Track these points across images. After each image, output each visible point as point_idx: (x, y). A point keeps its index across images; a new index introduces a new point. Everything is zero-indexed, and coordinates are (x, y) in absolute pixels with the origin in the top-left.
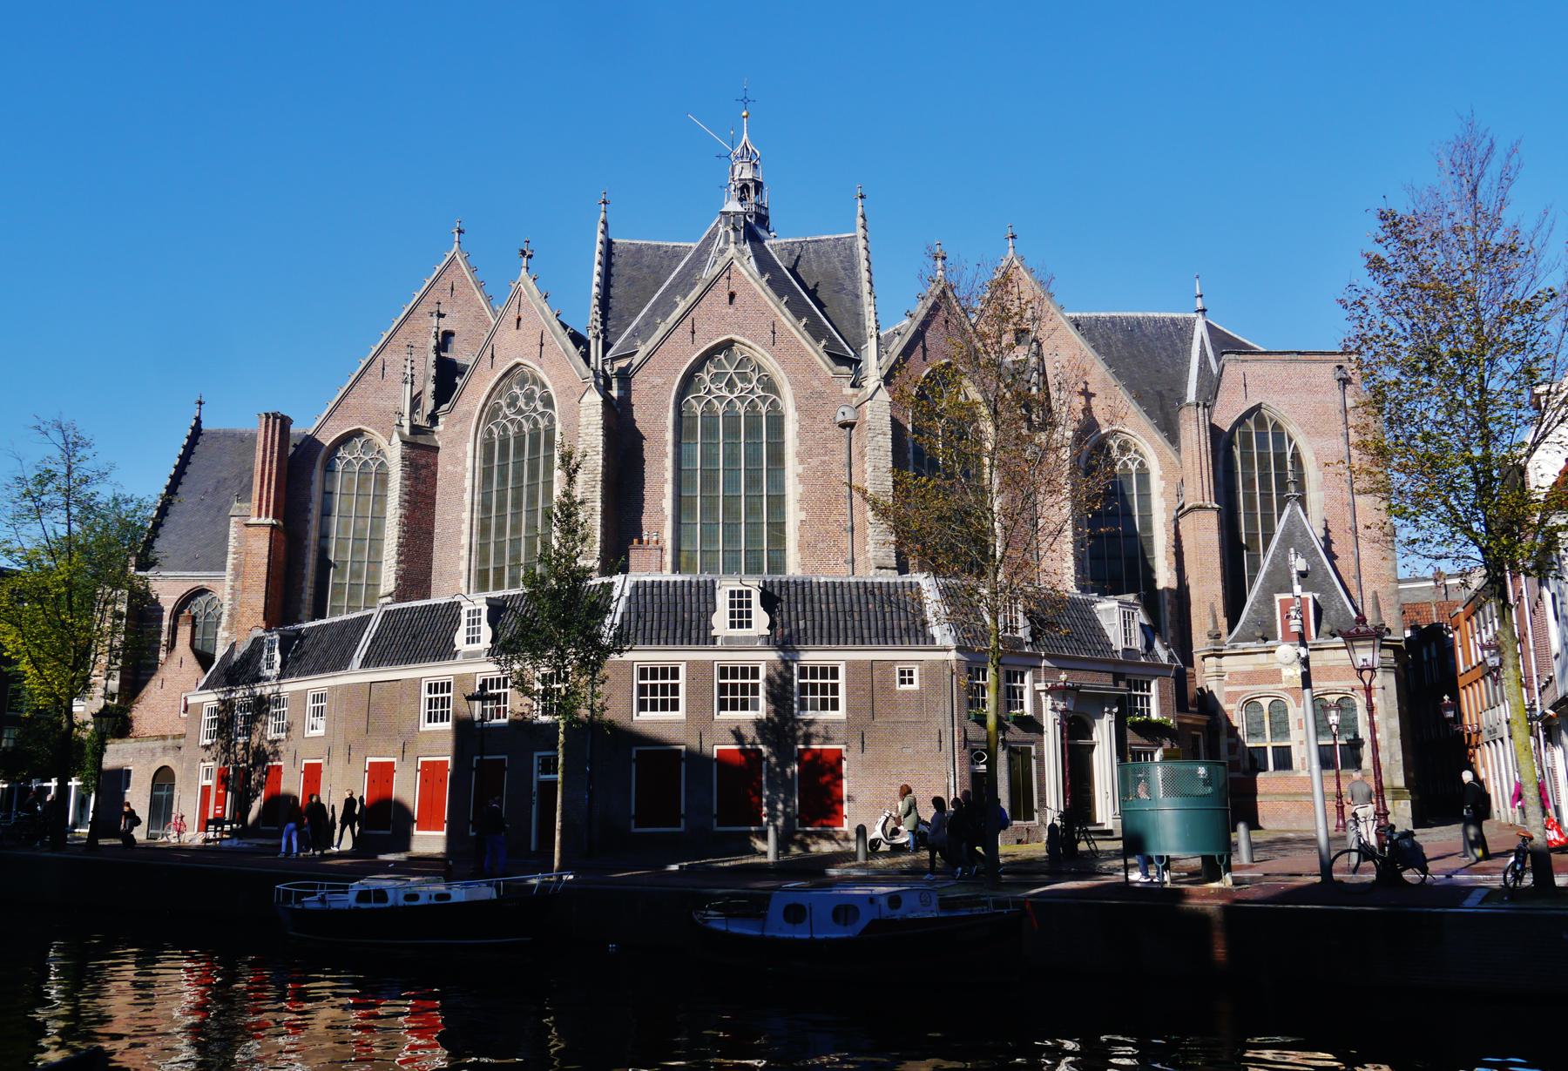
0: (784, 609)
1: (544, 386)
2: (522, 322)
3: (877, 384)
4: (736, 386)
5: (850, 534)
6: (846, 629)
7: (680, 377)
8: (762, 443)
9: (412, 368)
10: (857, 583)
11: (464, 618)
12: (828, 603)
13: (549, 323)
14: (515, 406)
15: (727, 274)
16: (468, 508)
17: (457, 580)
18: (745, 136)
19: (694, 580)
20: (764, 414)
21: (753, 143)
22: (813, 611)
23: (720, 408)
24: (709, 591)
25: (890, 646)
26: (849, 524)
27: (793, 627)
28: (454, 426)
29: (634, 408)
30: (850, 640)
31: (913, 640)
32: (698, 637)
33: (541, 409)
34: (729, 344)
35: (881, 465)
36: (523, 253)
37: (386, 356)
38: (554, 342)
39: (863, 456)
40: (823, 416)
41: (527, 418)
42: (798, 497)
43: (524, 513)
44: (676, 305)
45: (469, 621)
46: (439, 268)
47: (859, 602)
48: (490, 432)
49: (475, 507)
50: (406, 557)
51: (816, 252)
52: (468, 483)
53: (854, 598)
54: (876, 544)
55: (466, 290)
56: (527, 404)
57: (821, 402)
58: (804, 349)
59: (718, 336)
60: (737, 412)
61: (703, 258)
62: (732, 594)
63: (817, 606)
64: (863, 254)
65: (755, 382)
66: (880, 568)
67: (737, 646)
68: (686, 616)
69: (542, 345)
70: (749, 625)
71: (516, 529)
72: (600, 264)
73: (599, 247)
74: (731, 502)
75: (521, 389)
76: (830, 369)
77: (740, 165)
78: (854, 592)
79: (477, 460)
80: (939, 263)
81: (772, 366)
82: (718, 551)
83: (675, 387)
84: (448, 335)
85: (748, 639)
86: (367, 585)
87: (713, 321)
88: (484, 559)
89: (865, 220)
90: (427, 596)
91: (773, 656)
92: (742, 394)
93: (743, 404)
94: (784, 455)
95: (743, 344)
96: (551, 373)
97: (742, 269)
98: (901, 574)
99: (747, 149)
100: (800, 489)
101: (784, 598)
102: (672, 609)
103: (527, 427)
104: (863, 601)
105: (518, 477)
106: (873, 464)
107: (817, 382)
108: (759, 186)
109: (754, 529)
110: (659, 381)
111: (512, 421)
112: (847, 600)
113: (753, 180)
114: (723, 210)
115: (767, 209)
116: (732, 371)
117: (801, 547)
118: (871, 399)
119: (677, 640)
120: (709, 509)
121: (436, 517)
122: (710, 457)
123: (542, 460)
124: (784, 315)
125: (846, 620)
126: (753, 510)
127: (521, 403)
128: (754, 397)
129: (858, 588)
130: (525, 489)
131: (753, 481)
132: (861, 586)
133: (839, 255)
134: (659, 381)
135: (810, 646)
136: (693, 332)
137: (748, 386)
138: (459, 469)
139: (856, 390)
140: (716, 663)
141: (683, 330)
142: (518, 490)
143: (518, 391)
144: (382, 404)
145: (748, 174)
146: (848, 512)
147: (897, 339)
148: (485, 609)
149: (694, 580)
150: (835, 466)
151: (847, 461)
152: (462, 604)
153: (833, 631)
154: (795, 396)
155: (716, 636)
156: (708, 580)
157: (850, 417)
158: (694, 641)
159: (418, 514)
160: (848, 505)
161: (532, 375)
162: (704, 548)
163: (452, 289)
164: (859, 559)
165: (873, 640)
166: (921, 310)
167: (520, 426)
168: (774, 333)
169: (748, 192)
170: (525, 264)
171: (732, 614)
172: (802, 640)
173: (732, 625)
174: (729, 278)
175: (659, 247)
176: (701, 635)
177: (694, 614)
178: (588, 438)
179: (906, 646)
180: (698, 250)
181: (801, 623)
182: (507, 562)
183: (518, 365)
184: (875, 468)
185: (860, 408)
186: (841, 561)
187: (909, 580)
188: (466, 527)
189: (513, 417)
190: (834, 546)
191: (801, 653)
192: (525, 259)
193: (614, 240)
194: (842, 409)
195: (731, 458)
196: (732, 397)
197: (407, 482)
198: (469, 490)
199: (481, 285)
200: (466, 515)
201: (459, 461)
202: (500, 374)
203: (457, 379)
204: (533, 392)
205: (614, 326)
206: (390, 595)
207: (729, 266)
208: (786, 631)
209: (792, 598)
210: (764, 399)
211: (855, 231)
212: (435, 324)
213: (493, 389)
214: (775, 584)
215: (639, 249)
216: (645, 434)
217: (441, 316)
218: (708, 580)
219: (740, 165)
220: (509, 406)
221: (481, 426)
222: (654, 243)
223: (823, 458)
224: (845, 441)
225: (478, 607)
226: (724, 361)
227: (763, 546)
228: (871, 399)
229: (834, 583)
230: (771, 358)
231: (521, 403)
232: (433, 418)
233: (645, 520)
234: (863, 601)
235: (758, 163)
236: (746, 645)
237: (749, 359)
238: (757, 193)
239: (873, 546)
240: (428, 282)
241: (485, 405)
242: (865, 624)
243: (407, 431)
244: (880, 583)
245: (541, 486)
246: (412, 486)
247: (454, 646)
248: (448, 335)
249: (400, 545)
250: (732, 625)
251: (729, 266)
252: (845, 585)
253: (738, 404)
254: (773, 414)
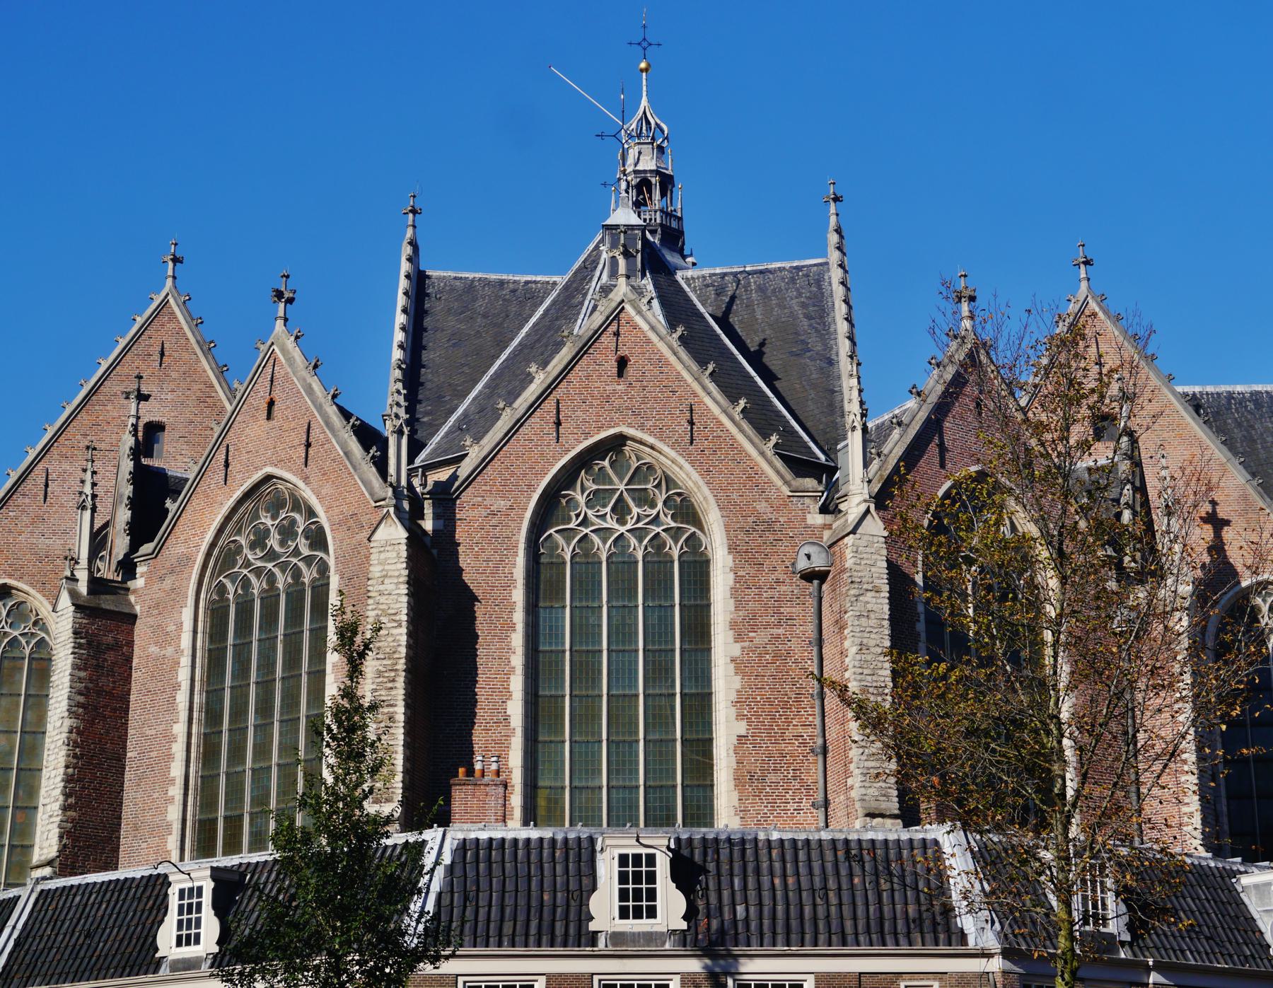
0: (712, 885)
1: (311, 513)
2: (276, 408)
3: (863, 507)
4: (630, 512)
5: (820, 758)
6: (815, 919)
7: (535, 497)
8: (673, 606)
9: (94, 484)
10: (833, 841)
11: (174, 902)
12: (784, 876)
13: (320, 408)
14: (263, 546)
15: (613, 328)
16: (183, 715)
17: (163, 838)
18: (644, 102)
19: (560, 837)
20: (676, 557)
21: (657, 112)
22: (759, 888)
23: (603, 549)
24: (585, 855)
25: (891, 949)
26: (820, 741)
27: (727, 916)
28: (162, 579)
29: (461, 549)
30: (822, 938)
31: (929, 937)
32: (566, 934)
33: (306, 552)
34: (618, 442)
35: (872, 643)
36: (279, 295)
37: (53, 464)
38: (329, 441)
39: (842, 628)
40: (774, 560)
41: (283, 567)
42: (733, 697)
43: (276, 725)
44: (529, 379)
45: (181, 907)
46: (140, 320)
47: (837, 873)
48: (222, 589)
49: (195, 715)
50: (78, 798)
51: (761, 289)
52: (183, 675)
53: (829, 866)
54: (865, 775)
55: (186, 356)
56: (283, 543)
57: (771, 537)
58: (742, 450)
59: (600, 428)
60: (631, 555)
61: (575, 301)
62: (623, 860)
63: (765, 880)
64: (839, 291)
65: (660, 505)
66: (872, 815)
67: (631, 949)
68: (546, 897)
69: (308, 445)
70: (652, 913)
71: (262, 751)
72: (405, 311)
73: (403, 284)
74: (622, 705)
75: (274, 518)
76: (786, 482)
77: (636, 149)
78: (829, 855)
79: (200, 636)
80: (965, 308)
81: (689, 477)
82: (600, 788)
83: (528, 514)
84: (154, 430)
85: (650, 937)
86: (12, 847)
87: (591, 406)
88: (207, 800)
89: (842, 237)
90: (112, 865)
91: (694, 966)
92: (640, 525)
93: (640, 541)
94: (709, 625)
95: (641, 442)
96: (324, 492)
97: (638, 320)
98: (907, 825)
99: (648, 123)
100: (737, 682)
101: (711, 866)
102: (522, 886)
103: (282, 581)
104: (843, 872)
105: (267, 664)
106: (858, 641)
107: (764, 504)
108: (667, 182)
109: (659, 750)
110: (502, 504)
111: (258, 572)
112: (817, 871)
113: (657, 172)
114: (609, 222)
115: (680, 219)
116: (622, 487)
117: (739, 781)
118: (854, 532)
119: (532, 939)
120: (585, 717)
121: (131, 732)
122: (586, 631)
123: (306, 635)
124: (709, 394)
125: (815, 905)
126: (661, 718)
127: (273, 542)
128: (659, 530)
129: (835, 849)
130: (278, 685)
131: (659, 670)
132: (840, 846)
133: (800, 295)
134: (502, 504)
135: (754, 949)
136: (558, 423)
137: (649, 512)
138: (170, 651)
139: (829, 518)
140: (596, 978)
141: (541, 422)
142: (266, 686)
143: (269, 522)
144: (42, 543)
145: (648, 163)
146: (818, 721)
147: (896, 433)
148: (208, 886)
149: (560, 837)
150: (794, 644)
151: (814, 635)
152: (171, 879)
153: (794, 923)
154: (727, 528)
155: (596, 933)
156: (584, 836)
157: (819, 562)
158: (559, 940)
159: (99, 727)
160: (817, 710)
161: (292, 495)
162: (576, 783)
163: (162, 354)
164: (837, 800)
165: (861, 938)
166: (934, 385)
167: (271, 579)
168: (691, 423)
169: (650, 192)
170: (281, 313)
171: (623, 895)
172: (742, 937)
173: (624, 913)
174: (617, 334)
175: (502, 283)
176: (572, 931)
177: (559, 895)
178: (383, 599)
179: (918, 948)
180: (566, 287)
181: (740, 909)
182: (247, 808)
183: (268, 478)
184: (862, 647)
185: (836, 548)
186: (805, 804)
187: (921, 836)
188: (178, 749)
189: (259, 564)
190: (795, 778)
191: (742, 960)
192: (282, 305)
193: (429, 273)
194: (806, 550)
195: (621, 632)
196: (622, 529)
197: (82, 674)
198: (185, 685)
199: (208, 348)
200: (180, 729)
201: (166, 638)
202: (238, 494)
203: (168, 503)
204: (293, 522)
205: (427, 414)
206: (49, 863)
207: (617, 314)
208: (715, 924)
209: (725, 868)
210: (675, 533)
211: (826, 257)
212: (133, 412)
213: (228, 518)
214: (696, 843)
215: (470, 286)
216: (478, 592)
217: (142, 397)
218: (584, 836)
219: (636, 149)
220: (253, 546)
221: (206, 580)
222: (493, 277)
223: (775, 631)
224: (811, 603)
225: (197, 884)
226: (610, 471)
227: (674, 778)
228: (854, 532)
229: (794, 841)
230: (687, 466)
231: (273, 542)
232: (127, 567)
233: (479, 737)
234: (843, 872)
235: (665, 144)
236: (647, 946)
237: (650, 467)
238: (663, 194)
239: (860, 778)
240: (123, 343)
241: (213, 545)
242: (846, 910)
243: (83, 588)
244: (873, 841)
245: (304, 678)
246: (91, 680)
247: (157, 950)
248: (154, 430)
249: (68, 779)
250: (624, 913)
251: (617, 314)
252: (813, 845)
253: (633, 541)
254: (691, 558)
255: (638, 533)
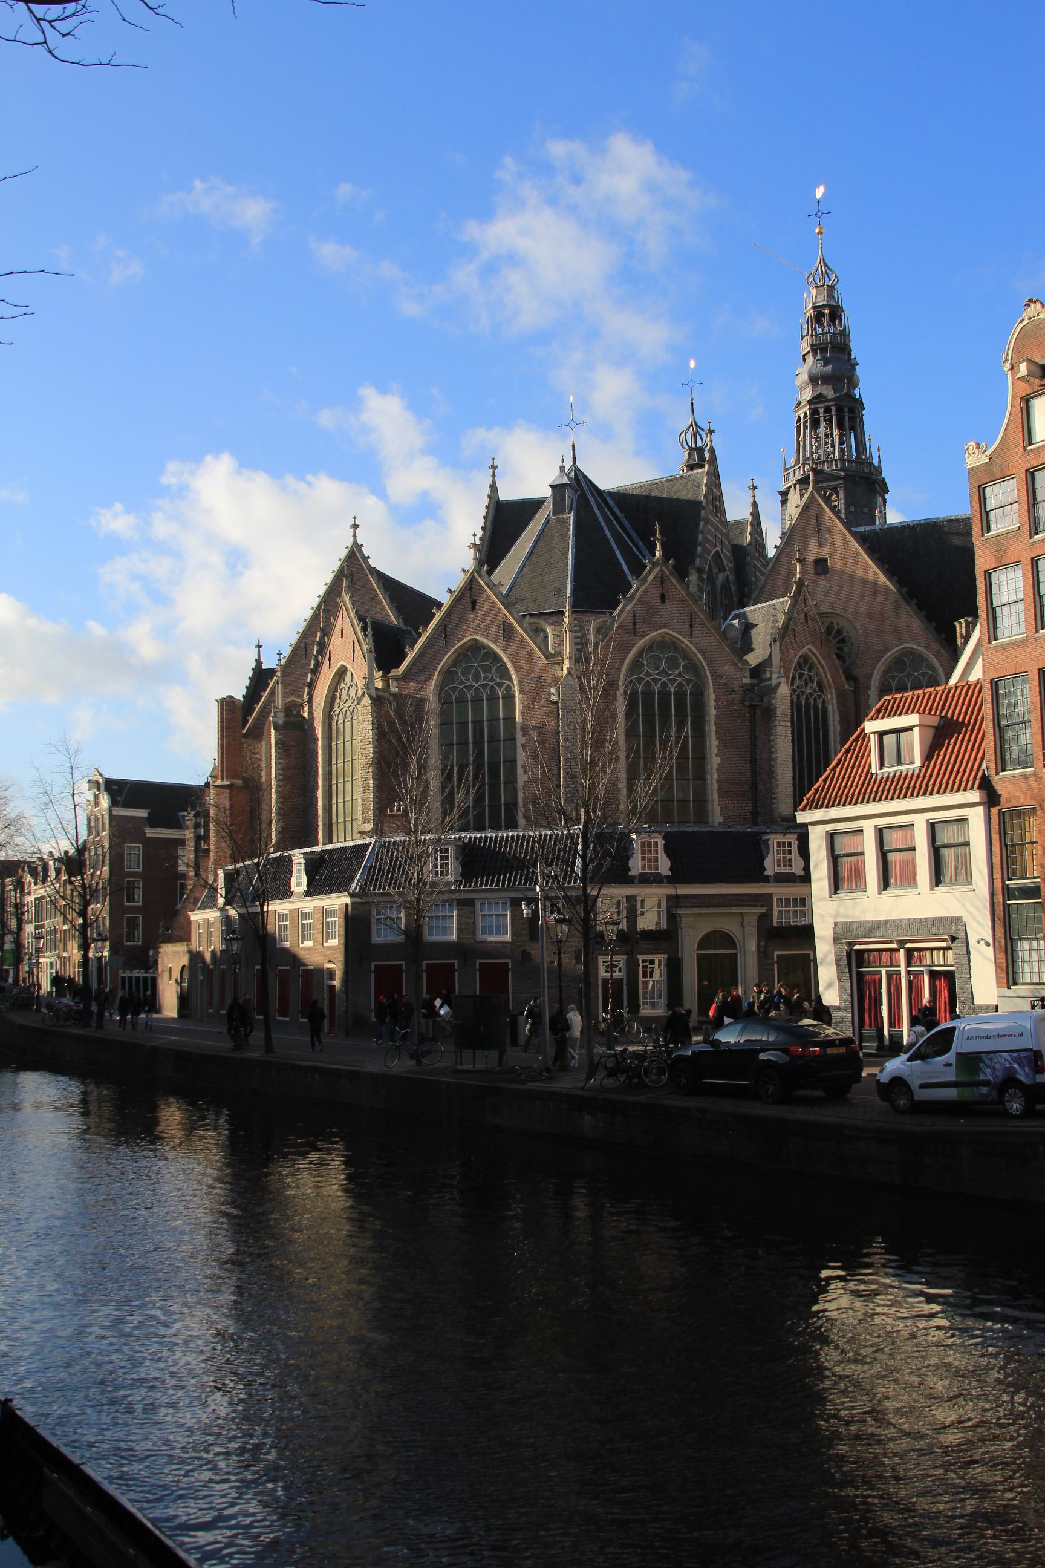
44: (434, 615)
116: (476, 664)
255: (484, 686)
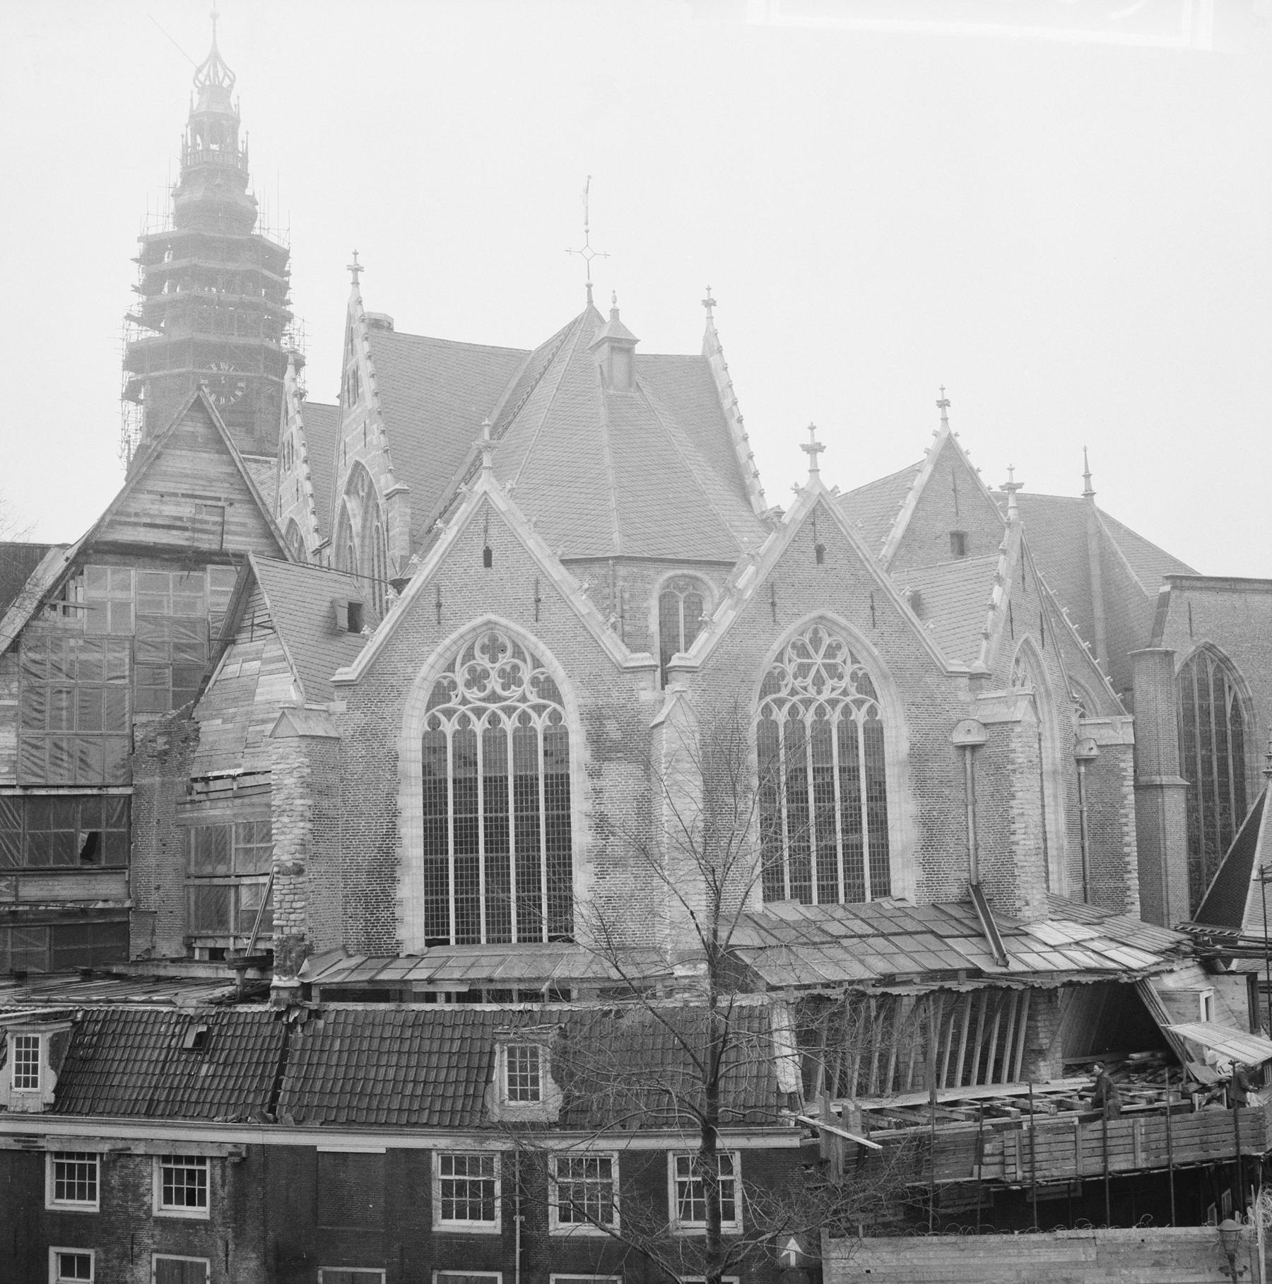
1: (537, 664)
56: (505, 687)
65: (847, 679)
92: (834, 695)
111: (479, 712)
127: (494, 684)
231: (494, 684)
255: (833, 703)
